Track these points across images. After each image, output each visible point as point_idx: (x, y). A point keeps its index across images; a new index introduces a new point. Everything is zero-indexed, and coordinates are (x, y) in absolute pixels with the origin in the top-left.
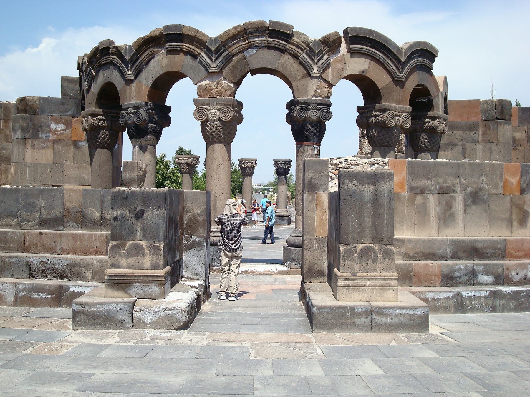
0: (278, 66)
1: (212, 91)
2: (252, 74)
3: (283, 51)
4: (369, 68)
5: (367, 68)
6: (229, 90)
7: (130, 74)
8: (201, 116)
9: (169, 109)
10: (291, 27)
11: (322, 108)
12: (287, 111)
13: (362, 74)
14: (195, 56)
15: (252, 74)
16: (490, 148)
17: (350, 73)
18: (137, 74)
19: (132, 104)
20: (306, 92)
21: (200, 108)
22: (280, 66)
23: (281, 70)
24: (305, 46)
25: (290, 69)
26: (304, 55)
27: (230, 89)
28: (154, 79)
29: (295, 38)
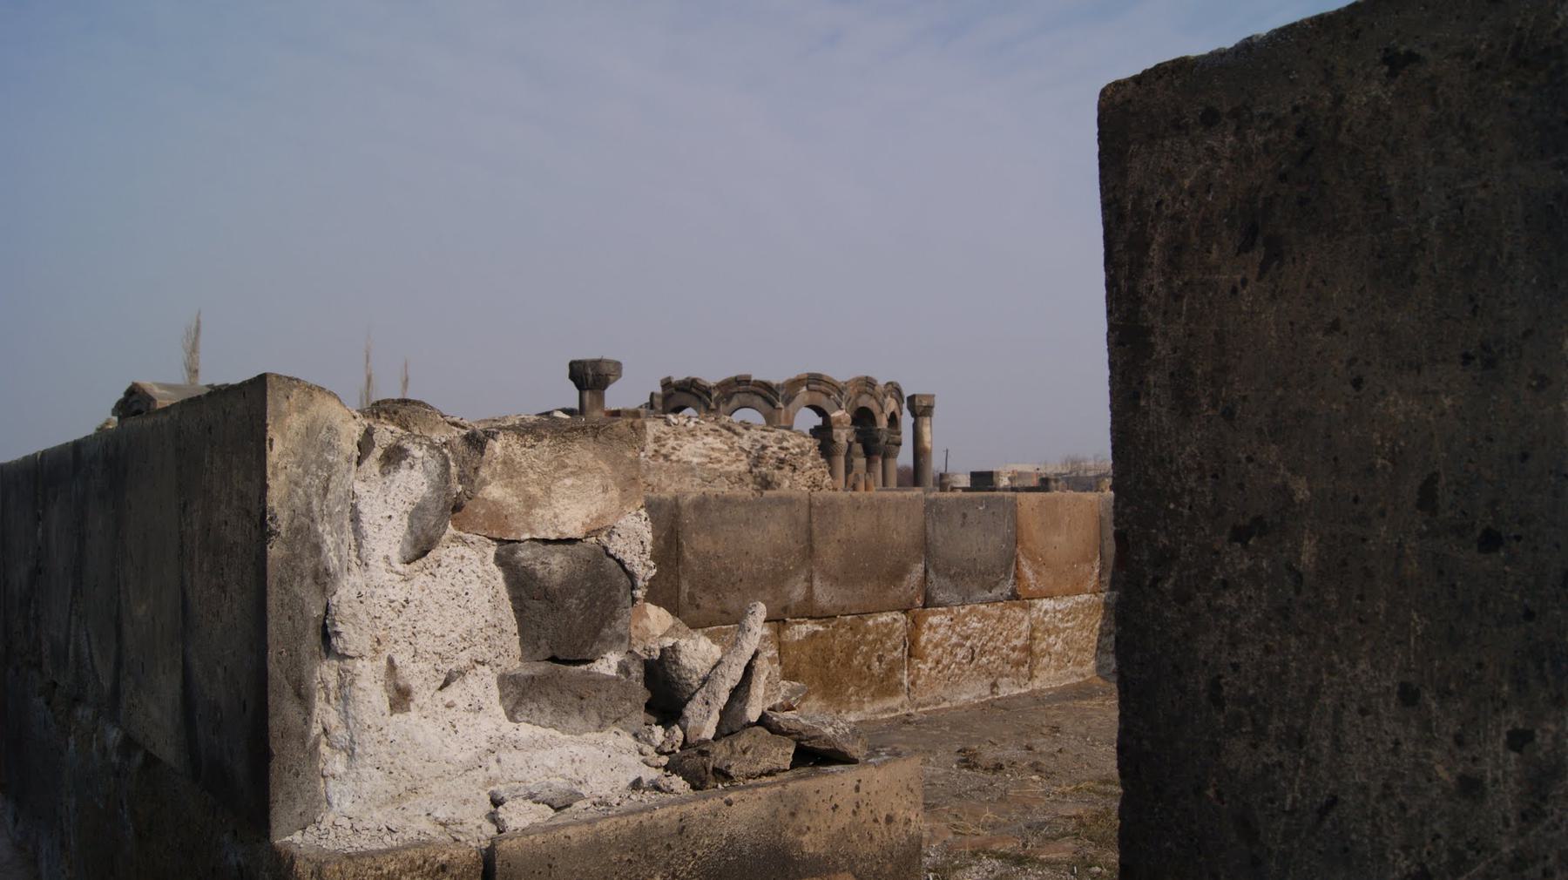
7: (780, 405)
10: (876, 381)
18: (787, 403)
29: (876, 388)
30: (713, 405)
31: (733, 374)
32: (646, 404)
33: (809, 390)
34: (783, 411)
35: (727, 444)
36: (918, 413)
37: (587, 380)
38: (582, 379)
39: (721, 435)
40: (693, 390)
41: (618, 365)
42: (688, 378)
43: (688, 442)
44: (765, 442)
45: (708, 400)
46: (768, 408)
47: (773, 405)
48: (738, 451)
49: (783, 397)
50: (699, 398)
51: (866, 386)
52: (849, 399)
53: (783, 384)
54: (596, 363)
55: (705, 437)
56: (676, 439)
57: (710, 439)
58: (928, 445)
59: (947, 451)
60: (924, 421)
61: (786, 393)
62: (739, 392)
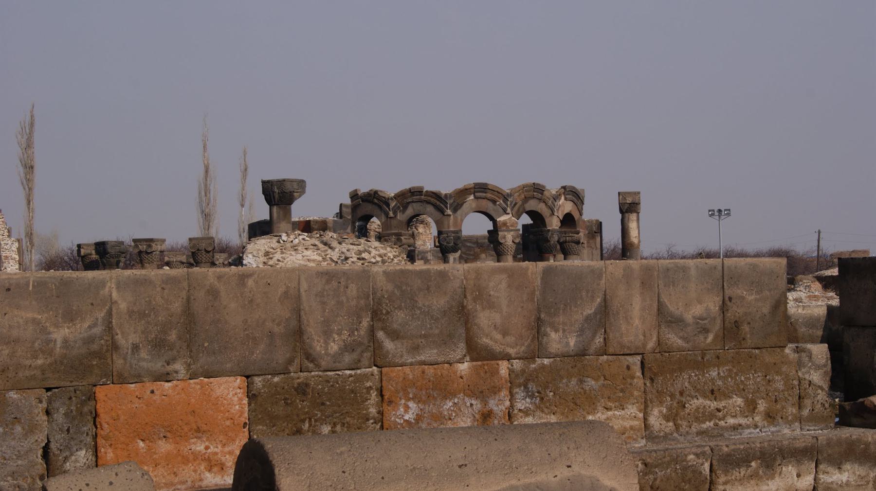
3: (540, 199)
7: (449, 212)
10: (544, 187)
14: (494, 202)
16: (592, 252)
18: (455, 210)
19: (452, 231)
20: (551, 226)
23: (539, 212)
26: (550, 202)
29: (545, 193)
30: (391, 214)
31: (407, 186)
32: (337, 213)
33: (476, 198)
34: (452, 216)
35: (322, 256)
36: (624, 211)
37: (274, 197)
38: (270, 198)
39: (318, 249)
40: (376, 201)
41: (302, 184)
42: (371, 190)
43: (291, 255)
44: (348, 254)
45: (387, 209)
46: (438, 215)
47: (442, 212)
48: (329, 262)
49: (451, 205)
50: (380, 207)
51: (534, 191)
52: (516, 204)
53: (450, 195)
54: (281, 182)
55: (305, 251)
56: (282, 253)
57: (308, 253)
58: (635, 241)
59: (819, 232)
60: (631, 217)
61: (454, 202)
62: (413, 202)
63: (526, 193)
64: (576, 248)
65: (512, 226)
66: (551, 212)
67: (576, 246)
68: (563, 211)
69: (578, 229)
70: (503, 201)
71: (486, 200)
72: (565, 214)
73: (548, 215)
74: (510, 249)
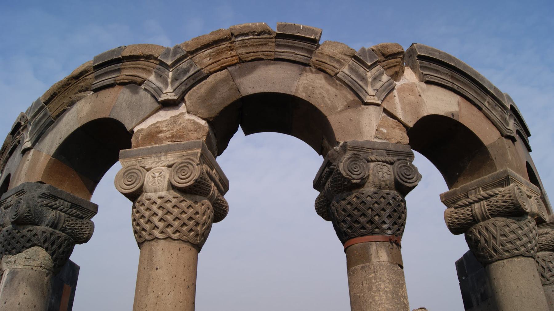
0: (297, 90)
1: (162, 134)
2: (247, 132)
4: (460, 110)
5: (457, 109)
6: (196, 131)
8: (130, 183)
9: (94, 209)
11: (398, 160)
12: (317, 193)
13: (452, 117)
15: (247, 132)
17: (432, 112)
20: (359, 131)
21: (130, 168)
22: (301, 89)
23: (302, 95)
24: (346, 58)
25: (320, 94)
27: (200, 128)
28: (63, 139)
51: (278, 46)
61: (45, 115)
63: (243, 51)
64: (513, 232)
65: (173, 137)
66: (351, 97)
67: (514, 226)
68: (415, 107)
69: (500, 170)
70: (159, 76)
71: (117, 88)
72: (426, 115)
73: (340, 104)
74: (160, 213)
